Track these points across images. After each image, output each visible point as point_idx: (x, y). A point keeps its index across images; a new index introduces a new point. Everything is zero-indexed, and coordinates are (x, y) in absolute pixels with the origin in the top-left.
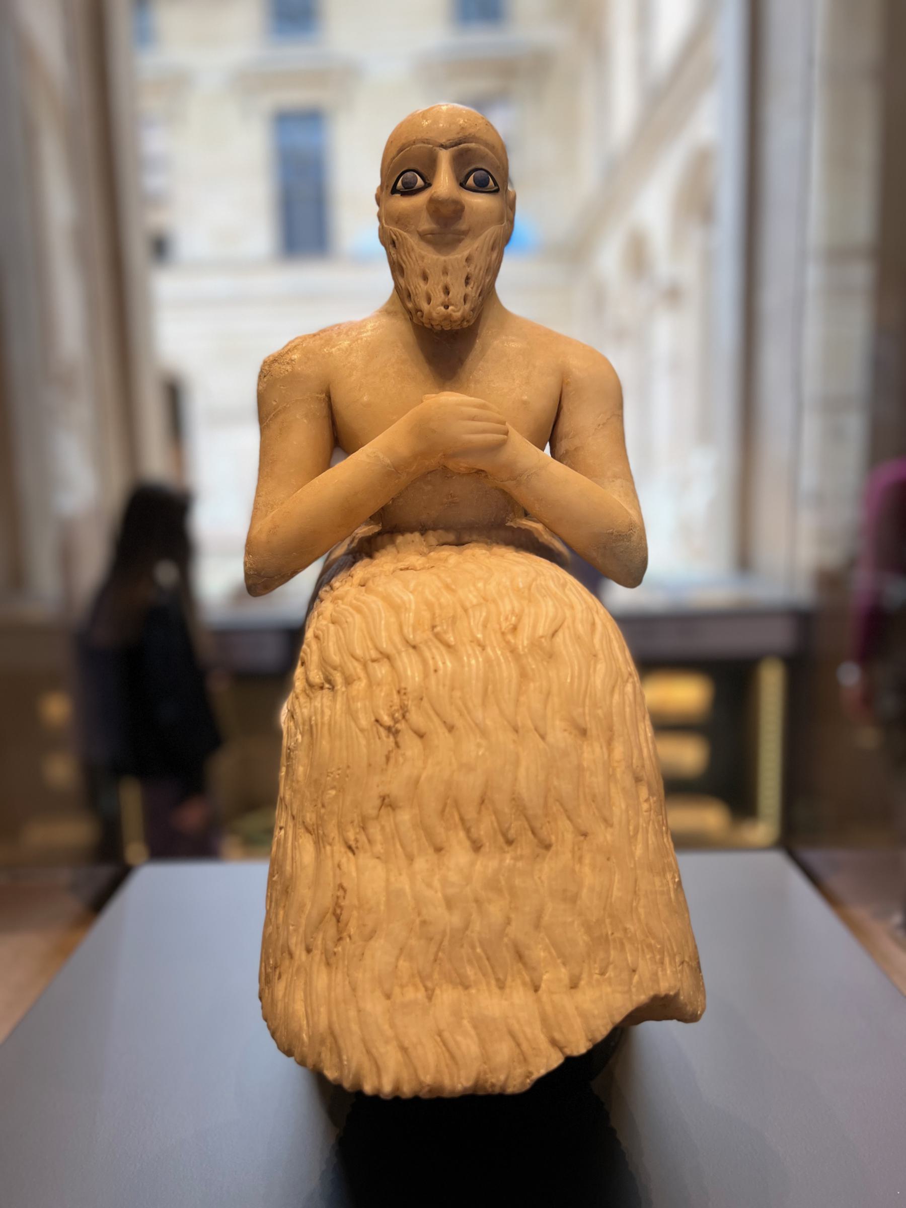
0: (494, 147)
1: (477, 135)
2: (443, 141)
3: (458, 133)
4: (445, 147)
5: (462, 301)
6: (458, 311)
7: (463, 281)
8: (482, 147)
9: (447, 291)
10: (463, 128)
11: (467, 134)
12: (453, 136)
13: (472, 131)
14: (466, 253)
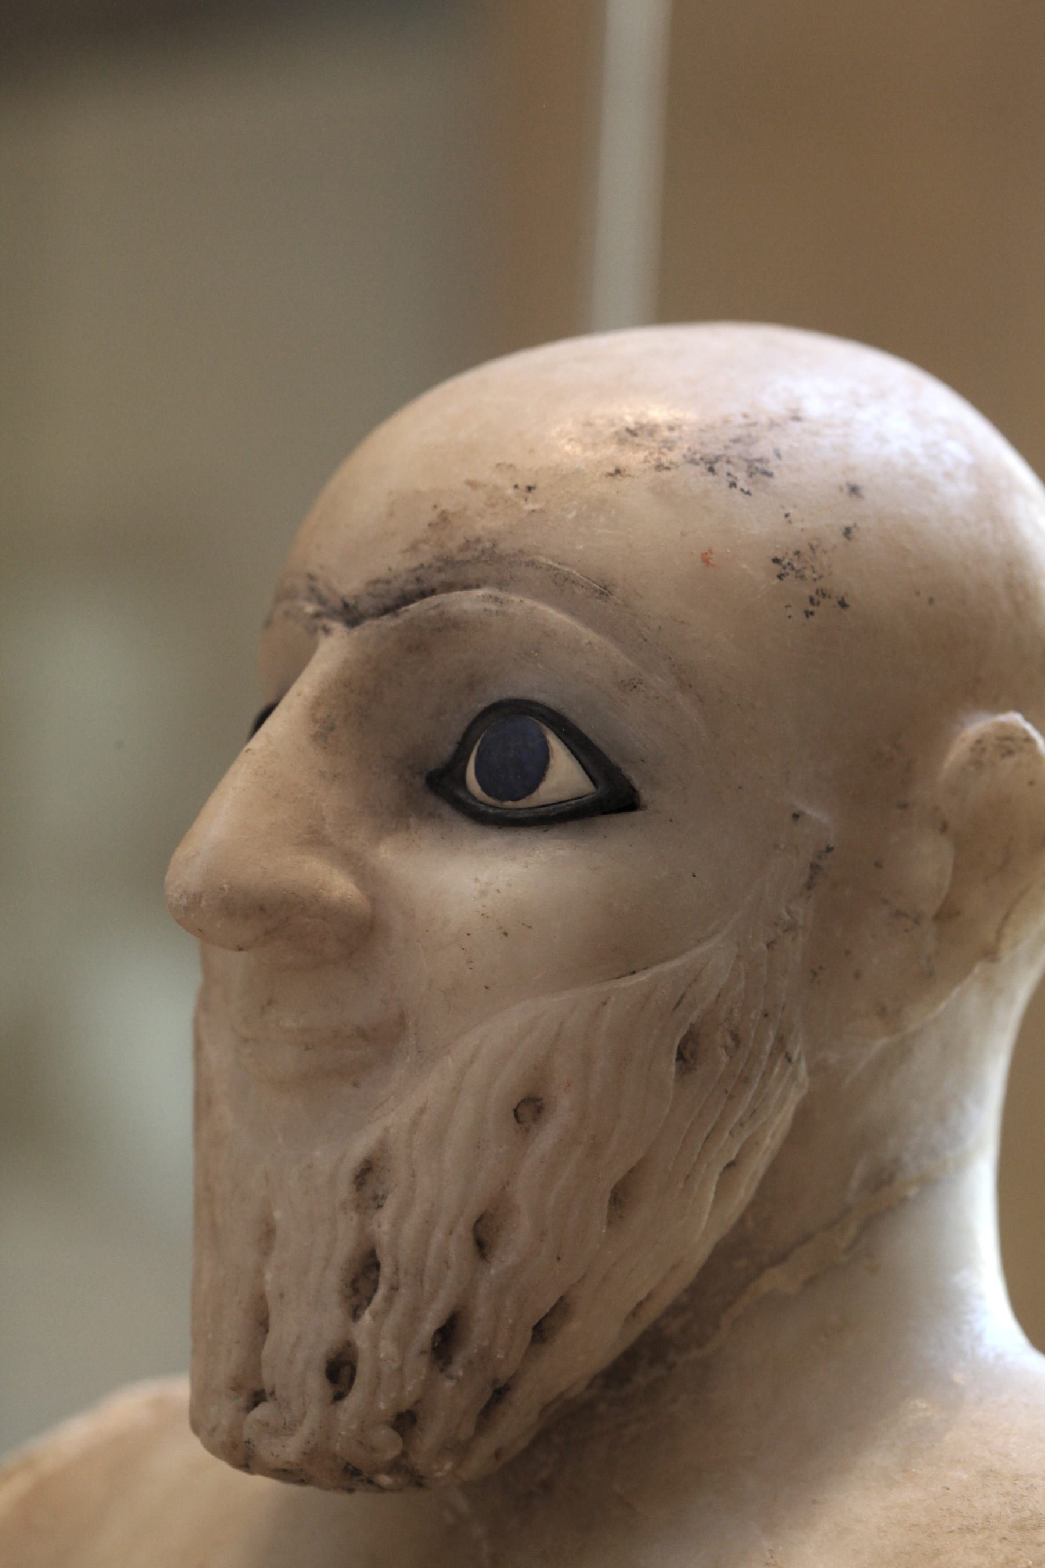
0: (604, 591)
1: (506, 546)
2: (350, 584)
3: (414, 548)
4: (351, 615)
5: (316, 1384)
6: (289, 1428)
7: (334, 1280)
8: (519, 603)
9: (261, 1323)
10: (444, 517)
11: (452, 546)
12: (393, 562)
13: (486, 524)
14: (360, 1147)
